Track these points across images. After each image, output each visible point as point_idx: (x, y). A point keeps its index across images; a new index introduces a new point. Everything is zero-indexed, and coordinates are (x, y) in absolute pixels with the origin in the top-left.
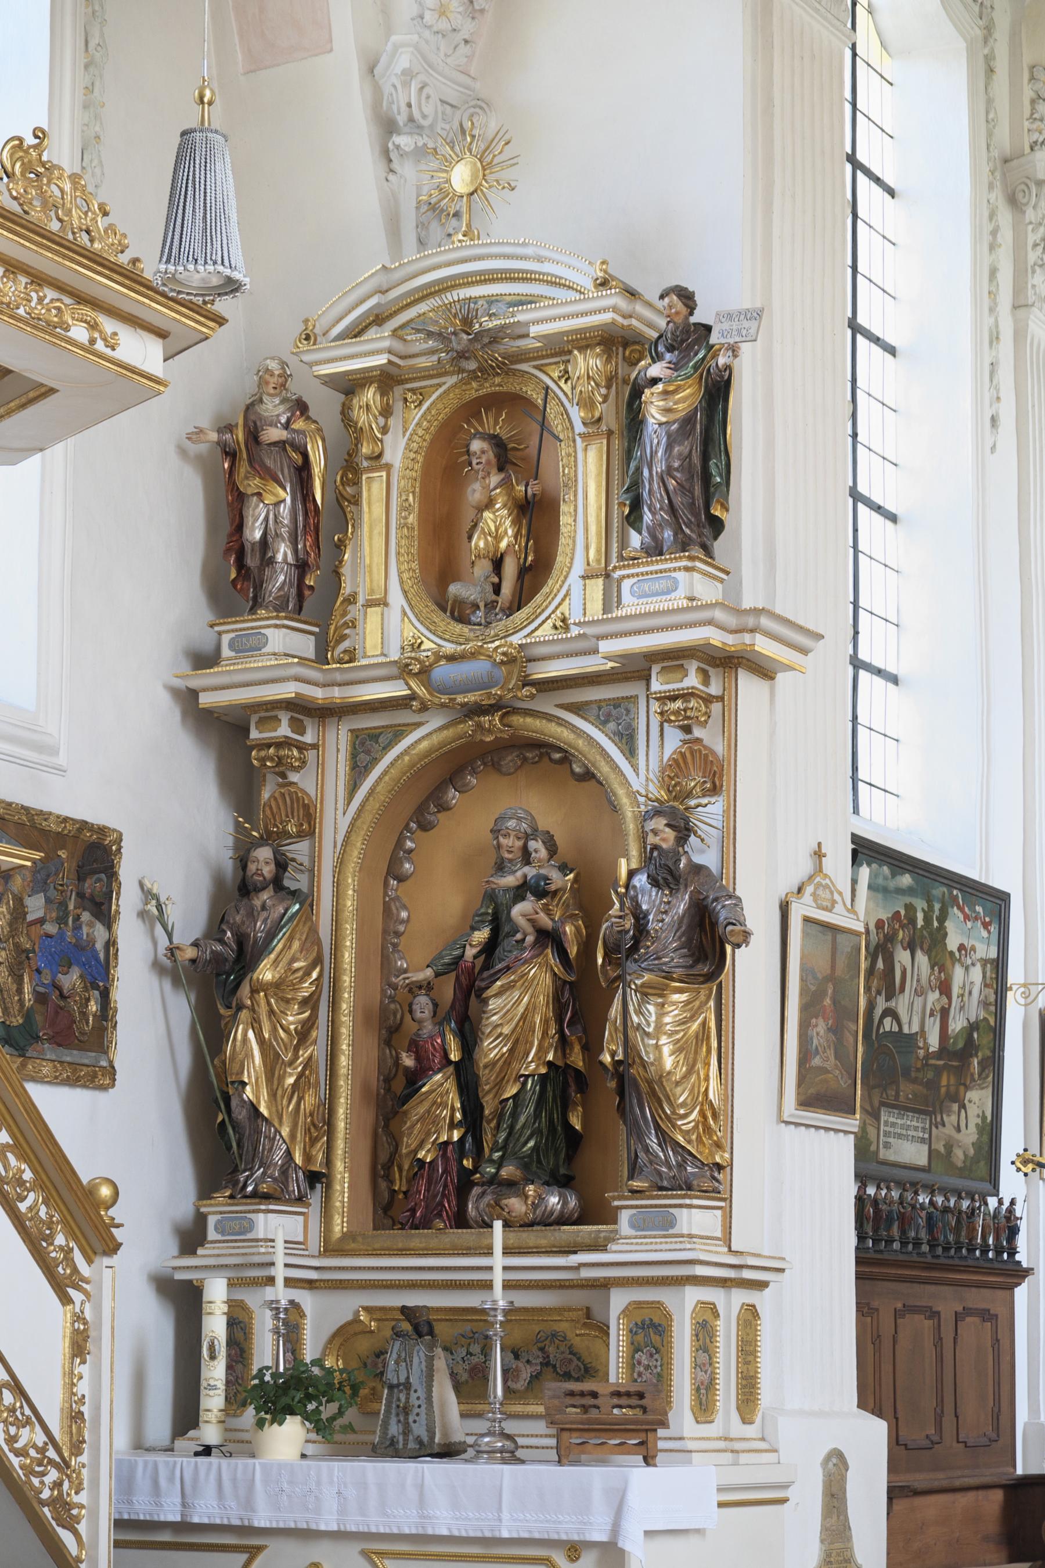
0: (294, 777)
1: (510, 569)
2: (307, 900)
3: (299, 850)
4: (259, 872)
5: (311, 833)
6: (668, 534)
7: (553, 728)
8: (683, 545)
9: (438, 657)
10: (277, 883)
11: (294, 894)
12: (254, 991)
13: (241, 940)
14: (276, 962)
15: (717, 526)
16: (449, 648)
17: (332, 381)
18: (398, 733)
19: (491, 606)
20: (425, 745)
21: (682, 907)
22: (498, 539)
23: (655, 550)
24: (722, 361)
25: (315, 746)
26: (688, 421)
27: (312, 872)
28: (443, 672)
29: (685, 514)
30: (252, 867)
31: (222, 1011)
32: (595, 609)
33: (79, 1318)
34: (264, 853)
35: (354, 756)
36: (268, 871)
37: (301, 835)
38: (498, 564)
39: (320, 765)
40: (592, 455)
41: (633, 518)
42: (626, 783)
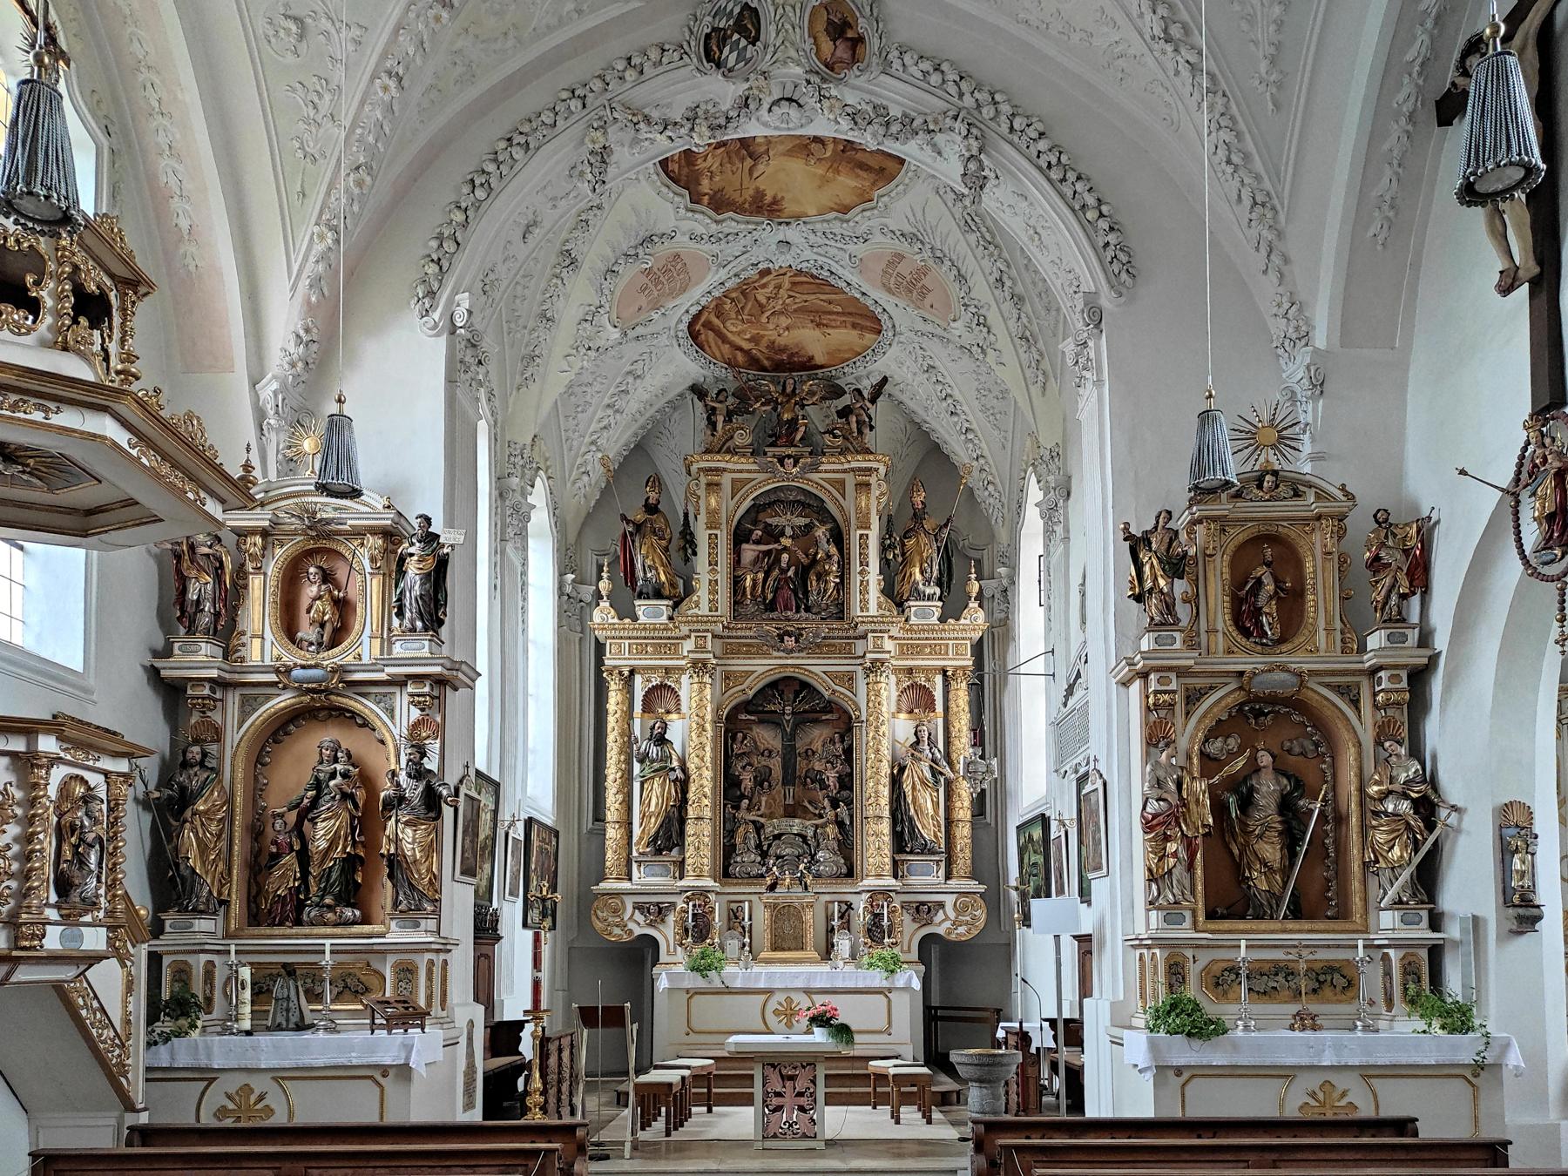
0: (209, 714)
1: (328, 628)
2: (217, 771)
3: (213, 748)
4: (193, 758)
5: (218, 741)
6: (419, 624)
7: (352, 703)
8: (426, 629)
9: (296, 665)
10: (202, 764)
11: (212, 769)
12: (194, 814)
13: (183, 789)
14: (206, 801)
15: (441, 623)
16: (299, 662)
17: (234, 530)
18: (268, 698)
19: (320, 644)
20: (282, 704)
21: (420, 789)
22: (324, 614)
23: (413, 630)
24: (445, 551)
25: (221, 700)
26: (429, 574)
27: (221, 759)
28: (297, 673)
29: (426, 616)
30: (189, 756)
31: (174, 823)
32: (376, 652)
33: (129, 974)
34: (196, 749)
35: (242, 705)
36: (198, 757)
37: (213, 741)
38: (322, 625)
39: (224, 709)
40: (375, 581)
41: (400, 614)
42: (390, 731)
